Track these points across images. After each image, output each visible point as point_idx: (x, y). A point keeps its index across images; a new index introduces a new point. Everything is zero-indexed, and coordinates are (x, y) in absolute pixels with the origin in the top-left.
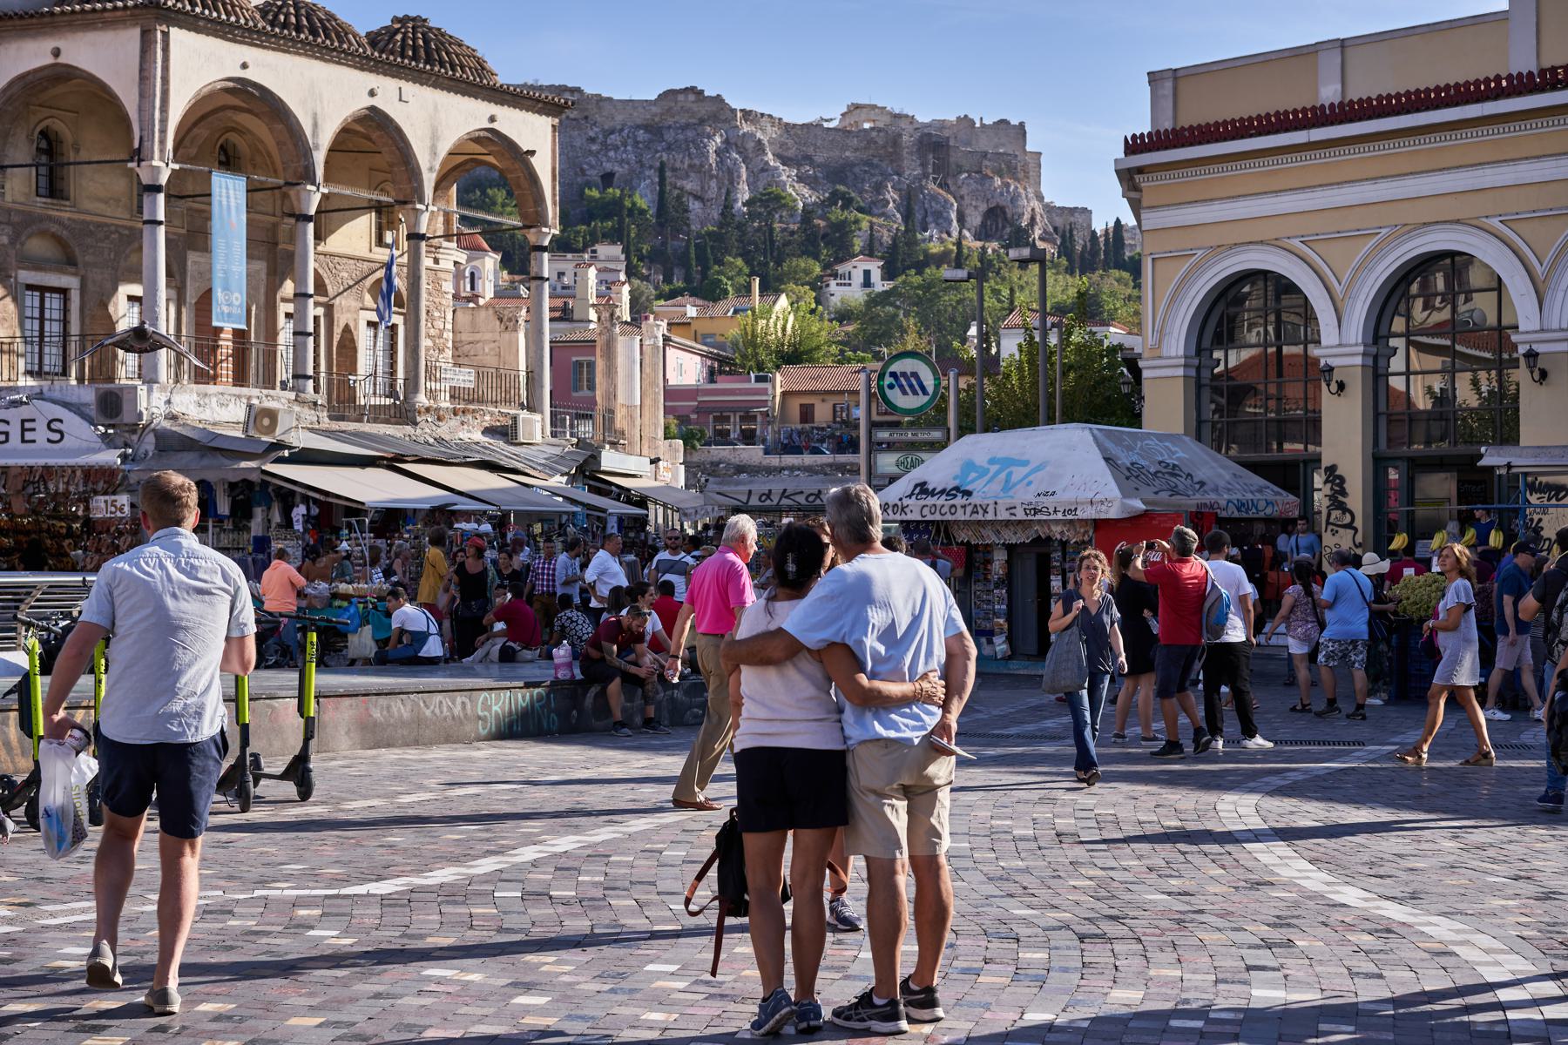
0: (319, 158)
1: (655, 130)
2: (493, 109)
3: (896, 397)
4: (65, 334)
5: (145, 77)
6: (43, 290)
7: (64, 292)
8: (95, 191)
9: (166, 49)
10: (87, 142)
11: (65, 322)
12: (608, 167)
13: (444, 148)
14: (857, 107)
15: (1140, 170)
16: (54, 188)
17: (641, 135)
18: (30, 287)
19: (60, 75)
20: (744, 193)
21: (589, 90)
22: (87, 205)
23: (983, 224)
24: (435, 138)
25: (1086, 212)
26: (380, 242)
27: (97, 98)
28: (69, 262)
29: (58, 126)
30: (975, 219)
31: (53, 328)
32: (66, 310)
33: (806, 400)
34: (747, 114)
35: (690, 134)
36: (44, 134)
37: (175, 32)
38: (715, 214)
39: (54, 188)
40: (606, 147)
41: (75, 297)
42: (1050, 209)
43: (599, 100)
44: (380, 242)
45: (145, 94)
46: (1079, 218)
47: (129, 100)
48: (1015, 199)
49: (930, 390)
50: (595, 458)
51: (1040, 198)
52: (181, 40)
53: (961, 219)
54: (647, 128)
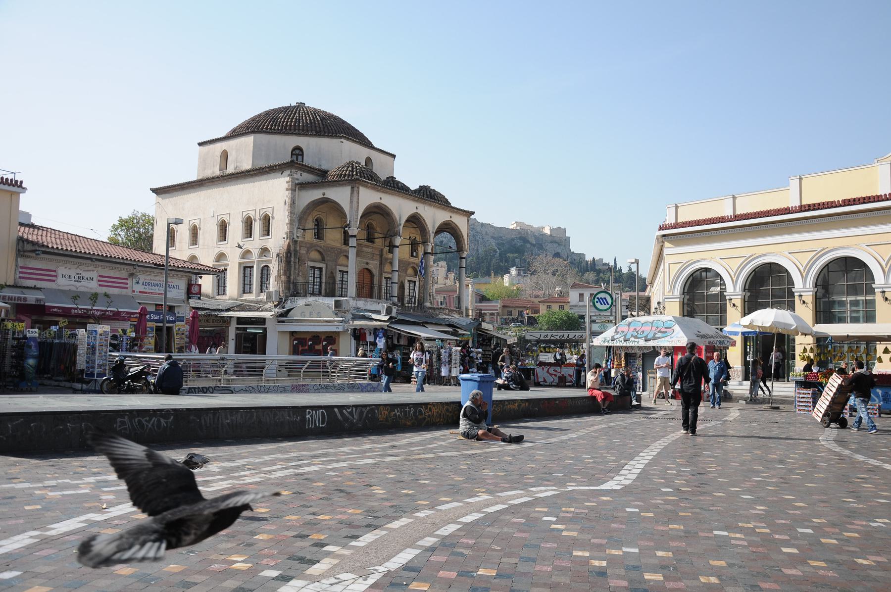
0: (401, 227)
2: (451, 214)
3: (598, 305)
4: (321, 282)
5: (351, 202)
6: (314, 268)
7: (321, 269)
8: (333, 237)
9: (358, 193)
10: (331, 221)
11: (321, 278)
13: (437, 225)
15: (664, 236)
16: (319, 235)
18: (311, 267)
19: (325, 201)
22: (329, 242)
24: (434, 223)
25: (584, 255)
26: (412, 255)
27: (335, 208)
28: (323, 260)
29: (323, 216)
31: (317, 280)
32: (321, 274)
33: (520, 309)
34: (482, 224)
36: (316, 220)
37: (361, 188)
39: (319, 235)
41: (324, 270)
44: (412, 255)
45: (351, 207)
47: (347, 209)
49: (610, 301)
50: (480, 324)
52: (363, 191)
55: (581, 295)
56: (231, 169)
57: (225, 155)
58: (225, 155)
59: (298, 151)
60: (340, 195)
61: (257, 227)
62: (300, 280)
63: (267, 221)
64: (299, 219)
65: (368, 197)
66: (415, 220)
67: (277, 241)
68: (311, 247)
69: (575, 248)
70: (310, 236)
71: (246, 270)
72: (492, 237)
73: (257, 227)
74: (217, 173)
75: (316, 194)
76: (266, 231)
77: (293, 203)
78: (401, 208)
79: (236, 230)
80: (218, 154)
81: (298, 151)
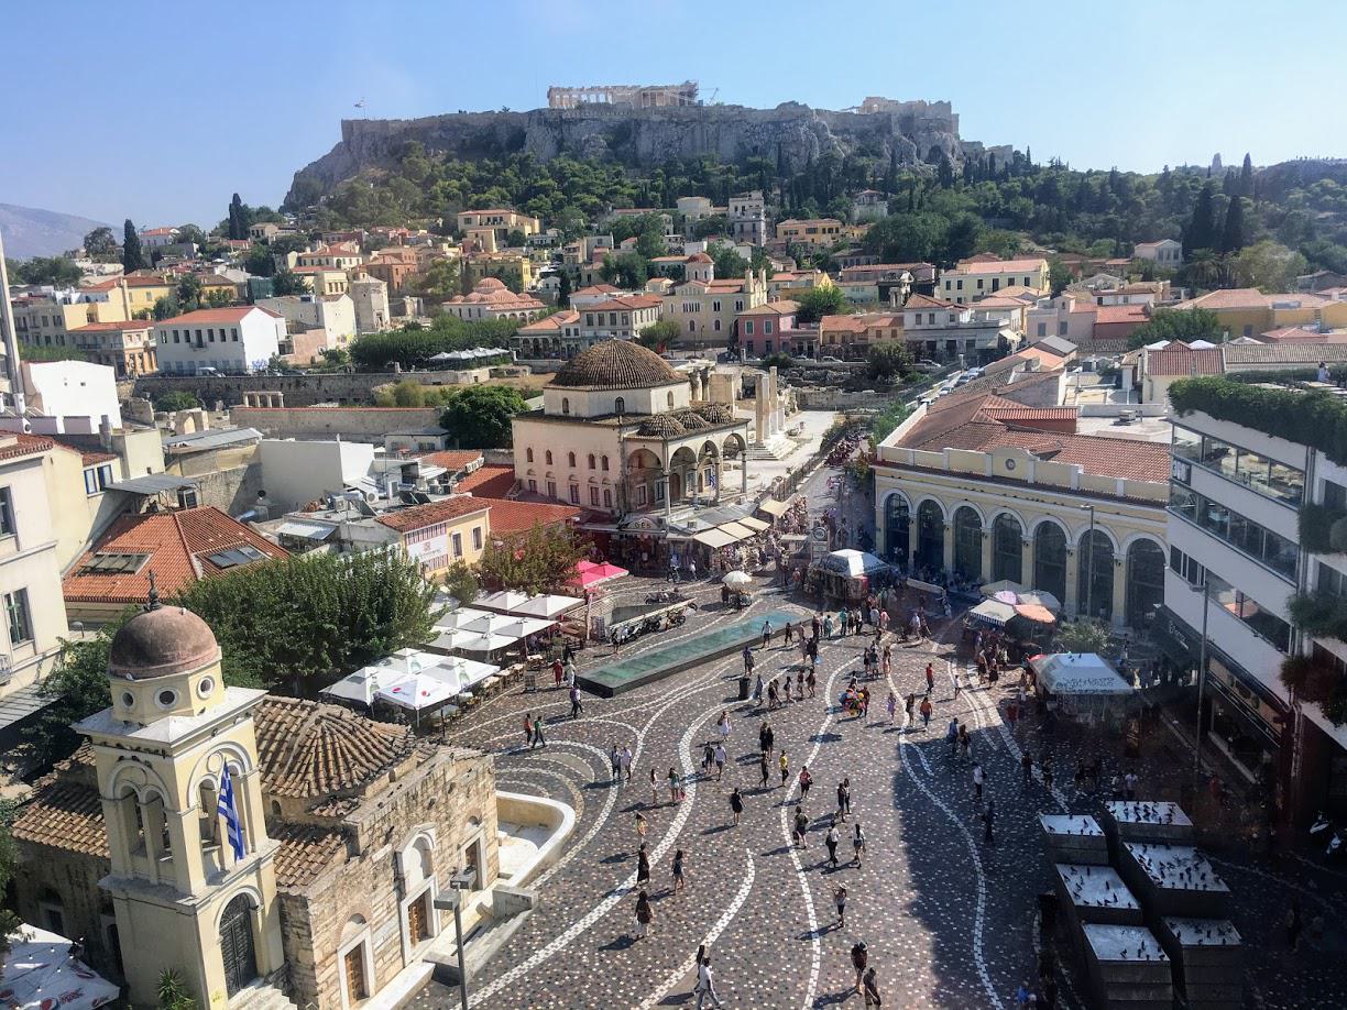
1: (777, 124)
12: (755, 143)
14: (869, 99)
17: (770, 127)
20: (816, 156)
21: (746, 106)
23: (930, 156)
30: (925, 153)
35: (792, 124)
38: (804, 163)
40: (753, 134)
42: (962, 144)
43: (751, 110)
46: (976, 147)
48: (945, 141)
51: (958, 137)
53: (918, 155)
54: (773, 123)
55: (919, 316)
56: (572, 413)
57: (566, 401)
58: (566, 401)
59: (620, 401)
60: (656, 449)
61: (598, 462)
62: (632, 500)
63: (605, 460)
64: (628, 462)
65: (673, 448)
66: (708, 446)
67: (615, 474)
68: (635, 475)
69: (967, 132)
70: (636, 470)
71: (594, 491)
72: (835, 132)
73: (598, 462)
74: (561, 411)
75: (639, 446)
76: (606, 468)
77: (623, 451)
78: (695, 444)
79: (582, 460)
80: (561, 399)
81: (620, 401)
